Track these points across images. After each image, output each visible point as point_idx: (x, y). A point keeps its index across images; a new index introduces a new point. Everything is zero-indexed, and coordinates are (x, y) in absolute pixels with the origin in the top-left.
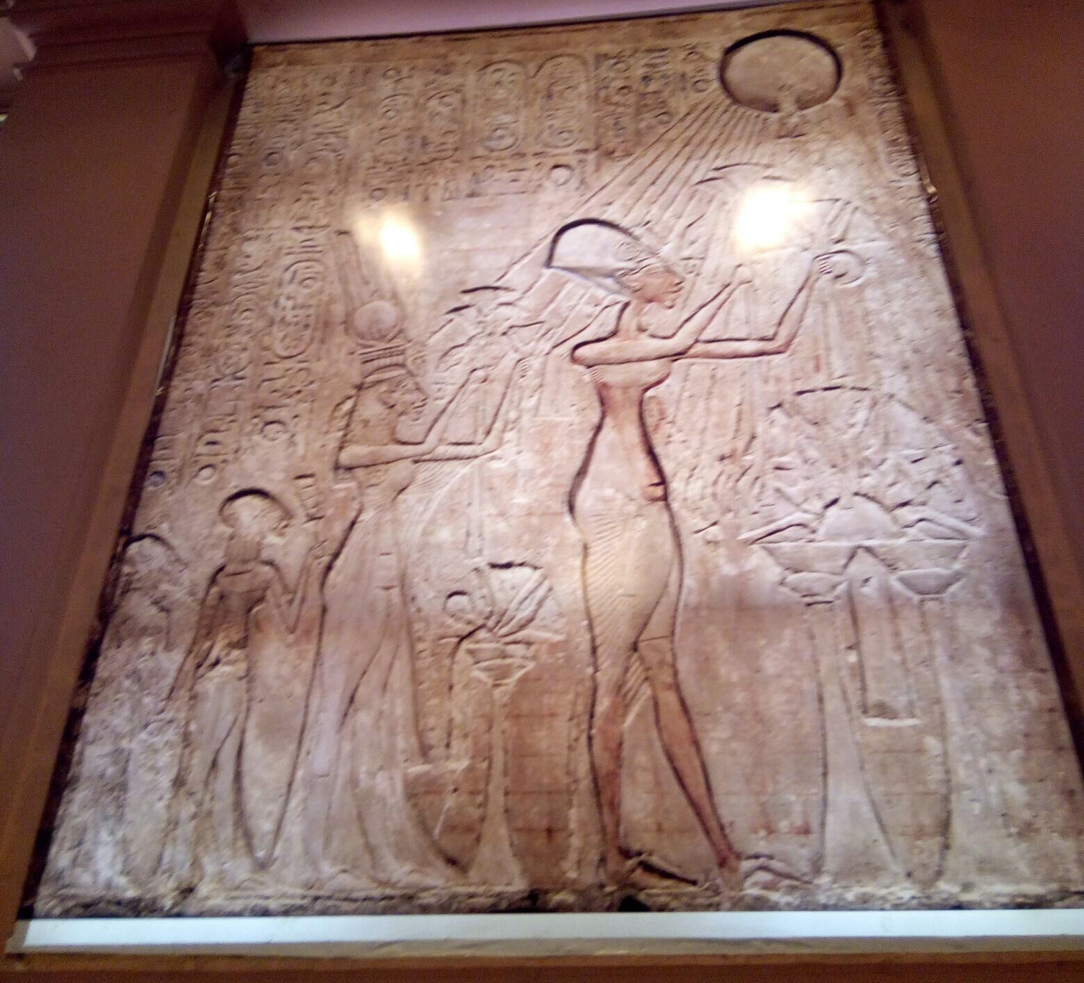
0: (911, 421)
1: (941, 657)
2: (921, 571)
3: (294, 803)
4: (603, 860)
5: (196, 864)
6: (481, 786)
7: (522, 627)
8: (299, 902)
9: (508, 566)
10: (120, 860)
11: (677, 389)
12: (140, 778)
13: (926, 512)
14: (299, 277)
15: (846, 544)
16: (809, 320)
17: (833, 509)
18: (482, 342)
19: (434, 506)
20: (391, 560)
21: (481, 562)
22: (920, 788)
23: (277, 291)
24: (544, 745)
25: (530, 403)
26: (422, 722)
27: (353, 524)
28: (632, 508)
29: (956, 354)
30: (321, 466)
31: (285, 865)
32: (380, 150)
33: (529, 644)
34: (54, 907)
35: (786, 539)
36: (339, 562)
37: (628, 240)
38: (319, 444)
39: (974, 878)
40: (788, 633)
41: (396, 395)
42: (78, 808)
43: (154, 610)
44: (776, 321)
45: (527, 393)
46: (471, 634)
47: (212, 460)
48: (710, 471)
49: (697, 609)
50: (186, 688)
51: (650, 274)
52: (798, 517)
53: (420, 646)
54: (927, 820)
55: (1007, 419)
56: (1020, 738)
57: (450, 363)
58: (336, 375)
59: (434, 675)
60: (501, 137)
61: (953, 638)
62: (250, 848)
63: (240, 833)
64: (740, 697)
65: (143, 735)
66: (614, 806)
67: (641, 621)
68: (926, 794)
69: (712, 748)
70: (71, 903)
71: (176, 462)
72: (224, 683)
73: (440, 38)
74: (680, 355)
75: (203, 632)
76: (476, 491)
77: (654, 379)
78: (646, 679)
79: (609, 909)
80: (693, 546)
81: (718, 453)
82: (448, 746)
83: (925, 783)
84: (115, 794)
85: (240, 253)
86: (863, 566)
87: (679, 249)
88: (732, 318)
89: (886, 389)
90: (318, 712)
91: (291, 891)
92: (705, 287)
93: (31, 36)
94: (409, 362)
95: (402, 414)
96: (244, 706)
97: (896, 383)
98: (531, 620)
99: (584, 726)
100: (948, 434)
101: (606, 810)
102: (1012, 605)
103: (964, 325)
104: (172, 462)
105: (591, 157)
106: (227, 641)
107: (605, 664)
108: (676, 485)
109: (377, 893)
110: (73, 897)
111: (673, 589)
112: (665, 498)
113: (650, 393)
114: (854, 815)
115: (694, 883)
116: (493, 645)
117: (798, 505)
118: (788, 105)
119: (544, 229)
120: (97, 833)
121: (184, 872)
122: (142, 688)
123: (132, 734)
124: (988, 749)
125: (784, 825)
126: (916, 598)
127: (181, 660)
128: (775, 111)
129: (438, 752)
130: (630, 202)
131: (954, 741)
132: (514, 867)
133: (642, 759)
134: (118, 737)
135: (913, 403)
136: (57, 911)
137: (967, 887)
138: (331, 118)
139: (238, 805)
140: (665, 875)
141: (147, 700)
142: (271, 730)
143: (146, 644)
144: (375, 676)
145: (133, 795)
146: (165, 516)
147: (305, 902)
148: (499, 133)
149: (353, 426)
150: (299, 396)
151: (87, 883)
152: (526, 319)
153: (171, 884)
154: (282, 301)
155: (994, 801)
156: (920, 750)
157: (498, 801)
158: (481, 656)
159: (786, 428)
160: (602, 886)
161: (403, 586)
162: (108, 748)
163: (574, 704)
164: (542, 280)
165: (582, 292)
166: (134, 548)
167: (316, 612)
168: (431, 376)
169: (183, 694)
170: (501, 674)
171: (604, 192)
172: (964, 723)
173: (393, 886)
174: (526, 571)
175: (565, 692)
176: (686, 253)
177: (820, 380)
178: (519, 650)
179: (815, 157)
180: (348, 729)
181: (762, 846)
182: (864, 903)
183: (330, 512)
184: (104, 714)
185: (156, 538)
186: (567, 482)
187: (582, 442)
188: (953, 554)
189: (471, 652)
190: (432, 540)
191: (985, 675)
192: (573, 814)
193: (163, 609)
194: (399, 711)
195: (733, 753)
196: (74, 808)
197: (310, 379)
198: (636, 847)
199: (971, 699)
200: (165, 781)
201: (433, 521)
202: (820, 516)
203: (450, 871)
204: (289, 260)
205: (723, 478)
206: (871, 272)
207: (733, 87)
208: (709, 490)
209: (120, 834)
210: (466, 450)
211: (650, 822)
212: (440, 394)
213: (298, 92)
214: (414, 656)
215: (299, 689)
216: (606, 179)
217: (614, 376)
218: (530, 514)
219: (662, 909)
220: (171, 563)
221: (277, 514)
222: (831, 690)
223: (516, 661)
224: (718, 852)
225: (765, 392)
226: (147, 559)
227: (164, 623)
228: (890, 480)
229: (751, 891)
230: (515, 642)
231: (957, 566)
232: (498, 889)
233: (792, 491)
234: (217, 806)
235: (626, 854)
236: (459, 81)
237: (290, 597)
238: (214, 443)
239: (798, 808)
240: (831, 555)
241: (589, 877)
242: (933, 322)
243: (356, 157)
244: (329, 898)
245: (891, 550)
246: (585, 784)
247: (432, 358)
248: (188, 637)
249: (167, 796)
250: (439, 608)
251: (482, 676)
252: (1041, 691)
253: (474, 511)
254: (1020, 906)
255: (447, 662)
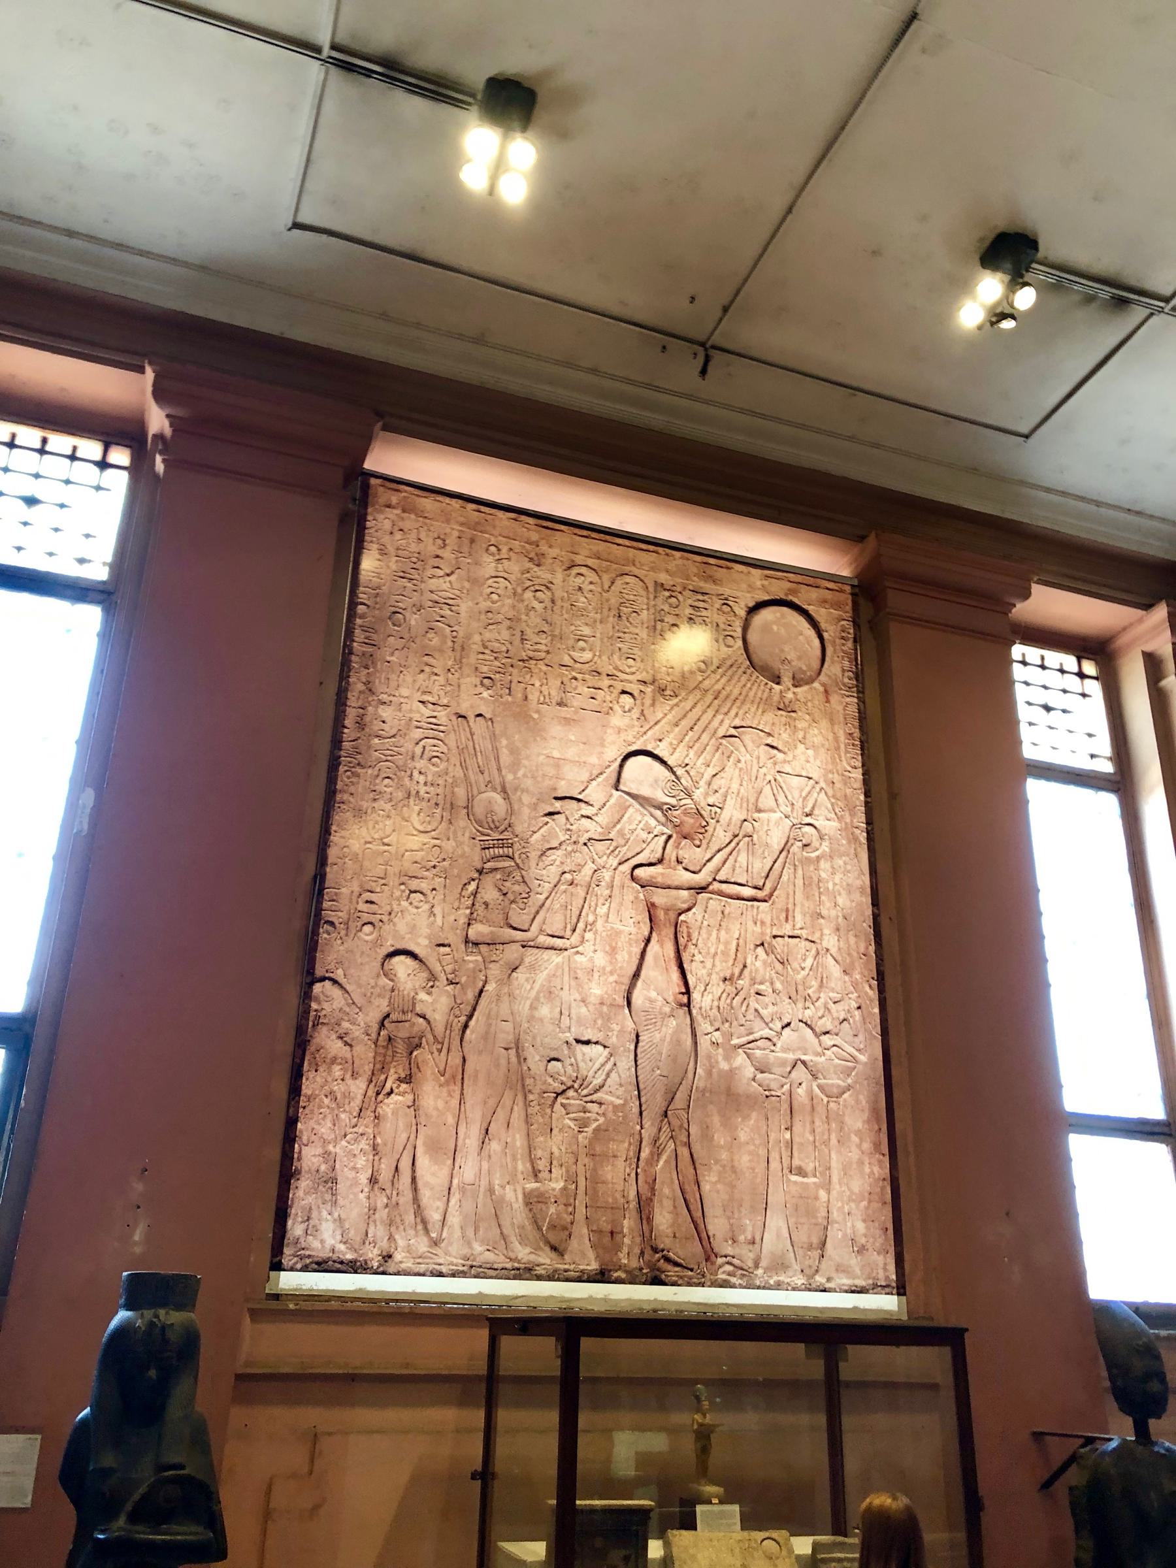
0: (835, 971)
1: (834, 1141)
2: (830, 1082)
3: (453, 1201)
4: (642, 1253)
5: (391, 1238)
6: (572, 1201)
7: (596, 1091)
8: (461, 1268)
9: (588, 1042)
10: (338, 1232)
11: (700, 918)
12: (344, 1174)
13: (837, 1040)
14: (427, 755)
15: (791, 1056)
16: (785, 878)
17: (787, 1030)
18: (569, 849)
19: (537, 986)
20: (508, 1027)
21: (570, 1037)
22: (813, 1221)
23: (411, 764)
24: (609, 1177)
25: (601, 910)
26: (533, 1152)
27: (481, 991)
28: (667, 1009)
29: (867, 926)
30: (455, 939)
31: (451, 1244)
32: (487, 635)
33: (600, 1104)
34: (296, 1263)
35: (758, 1048)
36: (472, 1023)
37: (673, 778)
38: (453, 918)
39: (834, 1275)
40: (754, 1115)
41: (507, 884)
42: (302, 1194)
43: (340, 1043)
44: (764, 874)
45: (601, 901)
46: (564, 1091)
47: (372, 918)
48: (717, 989)
49: (704, 1091)
50: (370, 1109)
51: (686, 813)
52: (766, 1032)
53: (531, 1097)
54: (815, 1241)
55: (889, 980)
56: (866, 1195)
57: (547, 863)
58: (462, 856)
59: (541, 1120)
60: (583, 650)
61: (841, 1129)
62: (426, 1230)
63: (418, 1220)
64: (724, 1155)
65: (344, 1143)
66: (650, 1220)
67: (670, 1096)
68: (816, 1224)
69: (706, 1188)
70: (308, 1261)
71: (343, 915)
72: (397, 1109)
73: (531, 521)
74: (703, 889)
75: (378, 1066)
76: (566, 978)
77: (685, 906)
78: (672, 1137)
79: (644, 1284)
80: (704, 1042)
81: (722, 975)
82: (550, 1171)
83: (816, 1218)
84: (330, 1184)
85: (377, 717)
86: (800, 1073)
87: (706, 794)
88: (737, 865)
89: (825, 944)
90: (464, 1140)
91: (455, 1261)
92: (722, 834)
93: (168, 416)
94: (516, 856)
95: (512, 902)
96: (414, 1127)
97: (830, 941)
98: (602, 1087)
99: (634, 1166)
100: (855, 985)
101: (644, 1222)
102: (874, 1111)
103: (875, 903)
104: (340, 914)
105: (649, 689)
106: (396, 1076)
107: (647, 1124)
108: (696, 996)
109: (509, 1266)
110: (309, 1256)
111: (690, 1075)
112: (688, 1005)
113: (682, 918)
114: (778, 1235)
115: (692, 1270)
116: (578, 1102)
117: (767, 1024)
118: (787, 681)
119: (614, 753)
120: (320, 1212)
121: (384, 1244)
122: (339, 1107)
123: (335, 1142)
124: (850, 1200)
125: (742, 1238)
126: (825, 1099)
127: (365, 1087)
128: (778, 683)
129: (544, 1175)
130: (675, 742)
131: (834, 1193)
132: (591, 1254)
133: (666, 1191)
134: (325, 1142)
135: (839, 958)
136: (299, 1266)
137: (829, 1280)
138: (446, 586)
139: (416, 1199)
140: (676, 1264)
141: (343, 1116)
142: (434, 1148)
143: (337, 1071)
144: (501, 1114)
145: (341, 1187)
146: (340, 963)
147: (465, 1269)
148: (581, 643)
149: (477, 906)
150: (434, 871)
151: (327, 1238)
152: (600, 834)
153: (376, 1251)
154: (416, 774)
155: (849, 1231)
156: (817, 1198)
157: (581, 1211)
158: (570, 1109)
159: (765, 962)
160: (641, 1269)
161: (518, 1048)
162: (320, 1151)
163: (628, 1150)
164: (612, 801)
165: (639, 818)
166: (317, 988)
167: (459, 1061)
168: (533, 870)
169: (369, 1114)
170: (583, 1124)
171: (657, 727)
172: (840, 1184)
173: (519, 1262)
174: (600, 1048)
175: (623, 1142)
176: (711, 801)
177: (787, 929)
178: (594, 1107)
179: (800, 735)
180: (485, 1153)
181: (729, 1250)
182: (778, 1286)
183: (463, 980)
184: (312, 1123)
185: (335, 982)
186: (627, 981)
187: (637, 950)
188: (848, 1072)
189: (563, 1105)
190: (537, 1014)
191: (855, 1155)
192: (626, 1222)
193: (346, 1043)
194: (518, 1144)
195: (718, 1192)
196: (300, 1193)
197: (442, 856)
198: (662, 1246)
199: (846, 1169)
200: (364, 1178)
201: (537, 999)
202: (779, 1034)
203: (553, 1255)
204: (418, 734)
205: (724, 995)
206: (825, 847)
207: (751, 649)
208: (716, 1003)
209: (336, 1215)
210: (558, 943)
211: (669, 1231)
212: (539, 890)
213: (414, 547)
214: (527, 1104)
215: (451, 1120)
216: (660, 715)
217: (660, 898)
218: (602, 1004)
219: (674, 1284)
220: (348, 1005)
221: (425, 975)
222: (774, 1156)
223: (593, 1116)
224: (705, 1252)
225: (754, 932)
226: (329, 999)
227: (349, 1056)
228: (820, 1014)
229: (722, 1276)
230: (592, 1102)
231: (849, 1081)
232: (581, 1267)
233: (764, 1012)
234: (402, 1200)
235: (655, 1250)
236: (549, 576)
237: (439, 1046)
238: (372, 902)
239: (750, 1228)
240: (783, 1063)
241: (634, 1264)
242: (857, 896)
243: (468, 637)
244: (480, 1267)
245: (816, 1064)
246: (633, 1205)
247: (534, 855)
248: (368, 1068)
249: (366, 1190)
250: (542, 1069)
251: (571, 1124)
252: (880, 1167)
253: (564, 994)
254: (853, 1292)
255: (548, 1111)
